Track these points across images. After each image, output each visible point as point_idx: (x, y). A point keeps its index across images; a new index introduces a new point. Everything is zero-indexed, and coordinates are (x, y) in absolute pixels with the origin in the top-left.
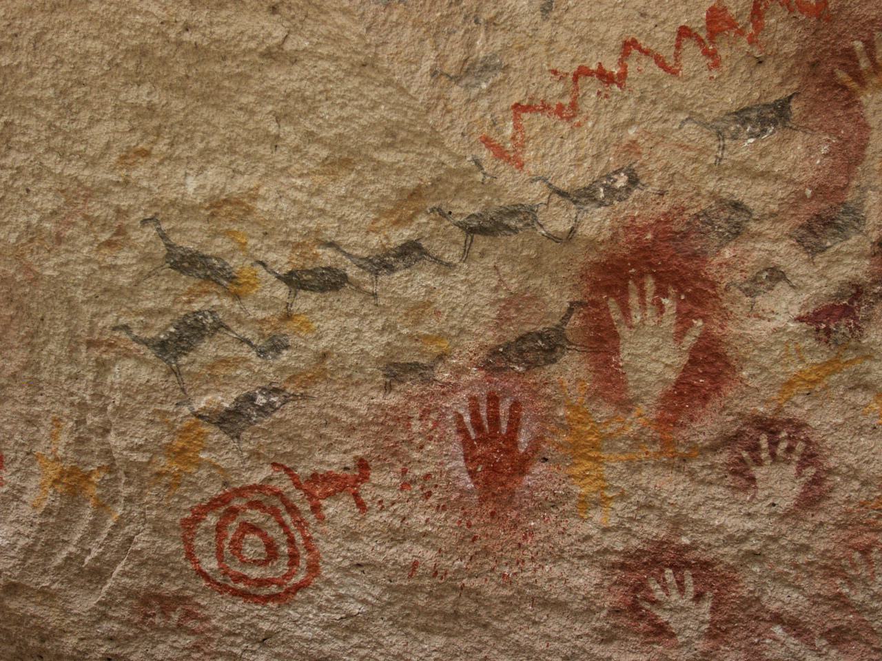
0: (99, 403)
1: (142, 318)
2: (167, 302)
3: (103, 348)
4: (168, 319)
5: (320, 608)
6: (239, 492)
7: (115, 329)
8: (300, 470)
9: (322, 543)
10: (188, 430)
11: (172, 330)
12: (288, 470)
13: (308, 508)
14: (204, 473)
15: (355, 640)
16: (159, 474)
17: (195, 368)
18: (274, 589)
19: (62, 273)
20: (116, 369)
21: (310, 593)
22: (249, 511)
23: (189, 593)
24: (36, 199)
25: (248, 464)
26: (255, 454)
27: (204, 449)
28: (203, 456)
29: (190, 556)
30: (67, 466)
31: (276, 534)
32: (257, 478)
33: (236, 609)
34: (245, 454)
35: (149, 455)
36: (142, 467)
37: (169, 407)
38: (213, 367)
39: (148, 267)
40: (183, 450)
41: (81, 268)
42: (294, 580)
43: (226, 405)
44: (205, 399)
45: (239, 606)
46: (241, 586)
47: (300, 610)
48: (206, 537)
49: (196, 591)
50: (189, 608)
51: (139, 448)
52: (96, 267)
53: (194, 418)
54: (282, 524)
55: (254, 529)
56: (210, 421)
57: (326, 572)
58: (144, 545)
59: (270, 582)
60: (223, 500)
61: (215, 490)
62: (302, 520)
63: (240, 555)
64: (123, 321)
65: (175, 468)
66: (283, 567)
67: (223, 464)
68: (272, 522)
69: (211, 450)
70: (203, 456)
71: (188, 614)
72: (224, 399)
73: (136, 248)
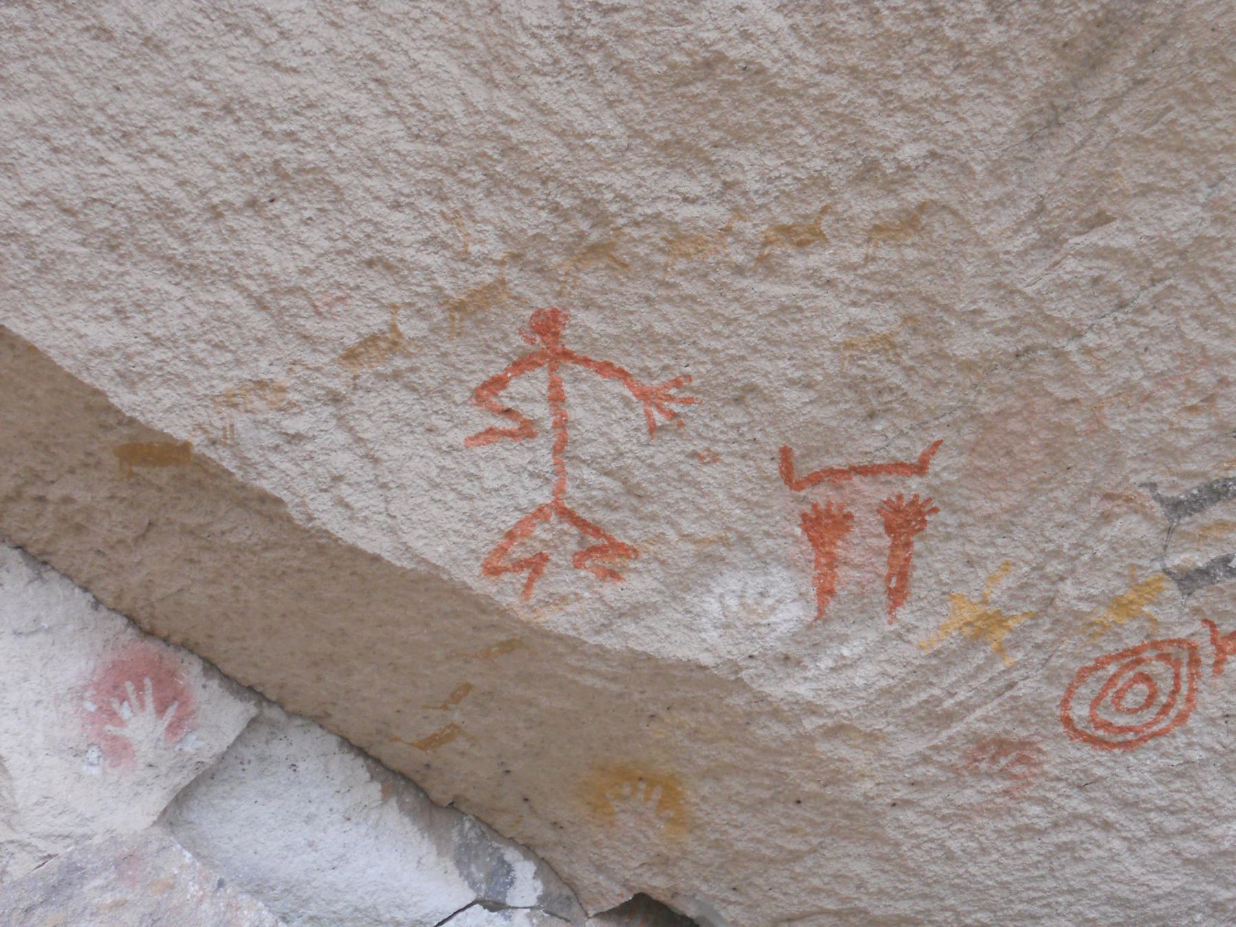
0: (1074, 553)
1: (1175, 478)
2: (1208, 467)
3: (1120, 502)
4: (1197, 482)
5: (1163, 755)
6: (1155, 645)
7: (1141, 485)
8: (1224, 627)
9: (1205, 695)
10: (1147, 584)
11: (1195, 492)
12: (1213, 626)
13: (1211, 662)
14: (1135, 625)
15: (1178, 784)
16: (1092, 624)
17: (1190, 529)
18: (1130, 736)
19: (1129, 429)
20: (1118, 523)
21: (1163, 740)
22: (1154, 662)
23: (1037, 738)
24: (1150, 358)
25: (1185, 618)
26: (1196, 611)
27: (1151, 602)
28: (1146, 609)
29: (1065, 703)
30: (991, 610)
31: (1166, 685)
32: (1182, 633)
33: (1079, 754)
34: (1187, 610)
35: (1094, 605)
36: (1078, 615)
37: (1145, 562)
38: (1209, 528)
39: (1214, 434)
40: (1131, 602)
41: (1151, 426)
42: (1155, 728)
43: (1200, 564)
44: (1182, 556)
45: (1087, 750)
46: (1101, 733)
47: (1141, 756)
48: (1093, 685)
49: (1045, 737)
50: (1026, 753)
51: (1090, 599)
52: (1166, 427)
53: (1161, 574)
54: (1177, 677)
55: (1146, 679)
56: (1173, 578)
57: (1193, 722)
58: (1028, 691)
59: (1130, 729)
60: (1135, 651)
61: (1133, 642)
62: (1197, 673)
63: (1118, 704)
64: (1155, 479)
65: (1111, 618)
66: (1148, 716)
67: (1160, 618)
68: (1169, 675)
69: (1159, 604)
70: (1146, 609)
71: (1021, 760)
72: (1197, 559)
73: (1217, 414)
